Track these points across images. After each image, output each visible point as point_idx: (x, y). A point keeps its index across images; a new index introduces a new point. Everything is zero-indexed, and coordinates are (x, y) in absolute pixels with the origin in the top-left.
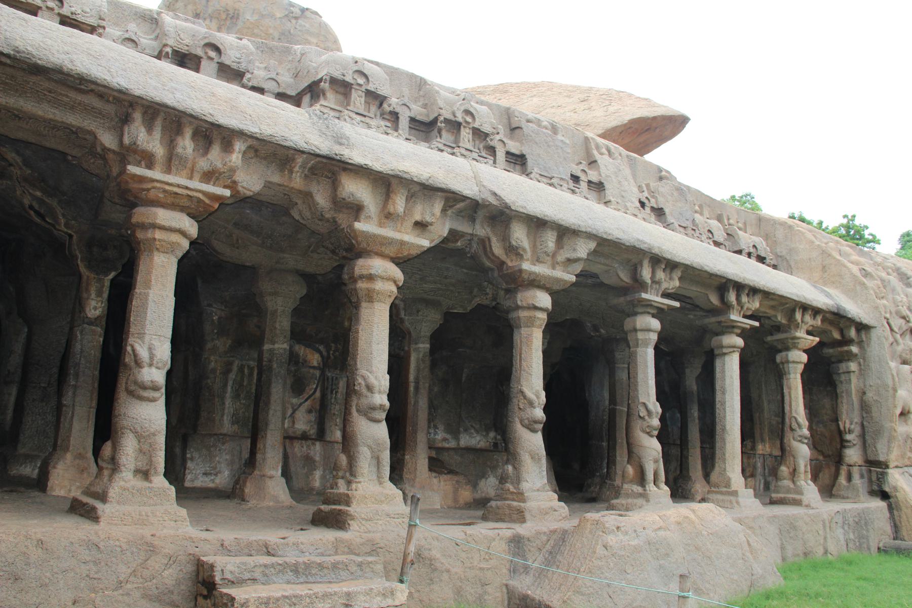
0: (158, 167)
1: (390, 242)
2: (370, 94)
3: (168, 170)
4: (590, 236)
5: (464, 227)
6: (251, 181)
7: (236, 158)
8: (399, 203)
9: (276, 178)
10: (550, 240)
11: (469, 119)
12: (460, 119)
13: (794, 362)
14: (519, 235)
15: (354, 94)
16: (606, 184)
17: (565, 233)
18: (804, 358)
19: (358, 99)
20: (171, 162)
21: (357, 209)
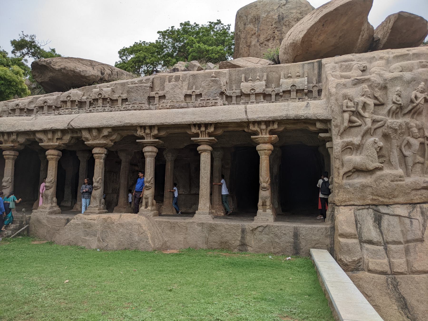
0: (4, 143)
1: (49, 146)
2: (72, 101)
3: (6, 144)
4: (107, 128)
5: (75, 135)
6: (21, 140)
7: (14, 137)
8: (50, 136)
9: (27, 137)
10: (95, 133)
11: (100, 96)
12: (97, 98)
13: (261, 150)
14: (85, 134)
15: (68, 103)
16: (166, 96)
17: (99, 129)
18: (269, 146)
19: (69, 104)
20: (6, 141)
21: (41, 140)
